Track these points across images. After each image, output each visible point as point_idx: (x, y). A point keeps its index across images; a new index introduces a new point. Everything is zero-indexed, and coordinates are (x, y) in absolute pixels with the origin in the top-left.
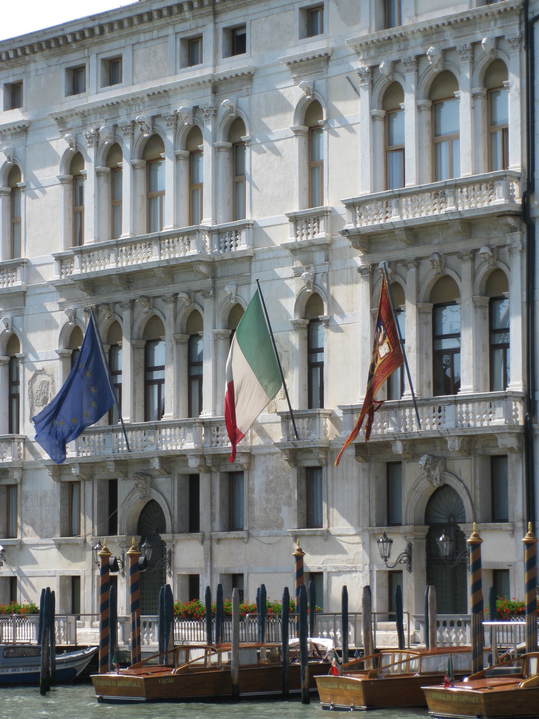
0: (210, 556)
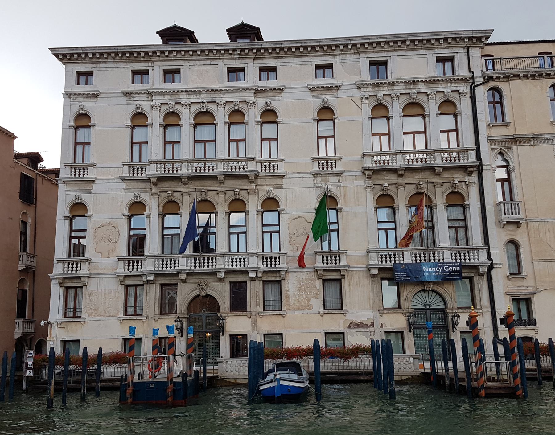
0: (254, 324)
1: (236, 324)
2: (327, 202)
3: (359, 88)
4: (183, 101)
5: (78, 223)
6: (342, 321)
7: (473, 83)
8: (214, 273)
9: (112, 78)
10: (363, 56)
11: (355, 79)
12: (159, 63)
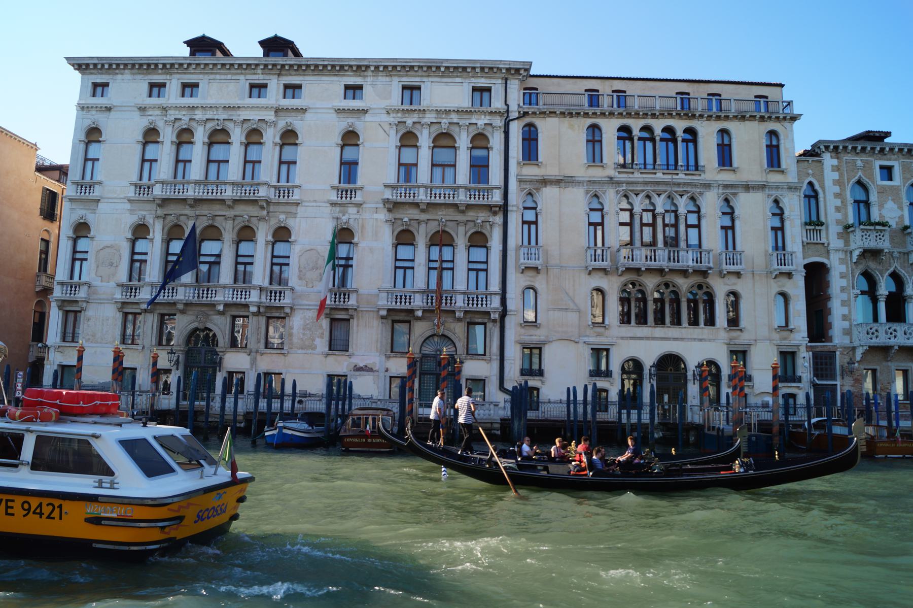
0: (253, 362)
1: (234, 361)
2: (344, 235)
3: (388, 113)
4: (197, 117)
5: (82, 244)
6: (346, 364)
7: (508, 116)
8: (213, 305)
9: (128, 90)
10: (396, 79)
11: (384, 103)
12: (178, 76)
